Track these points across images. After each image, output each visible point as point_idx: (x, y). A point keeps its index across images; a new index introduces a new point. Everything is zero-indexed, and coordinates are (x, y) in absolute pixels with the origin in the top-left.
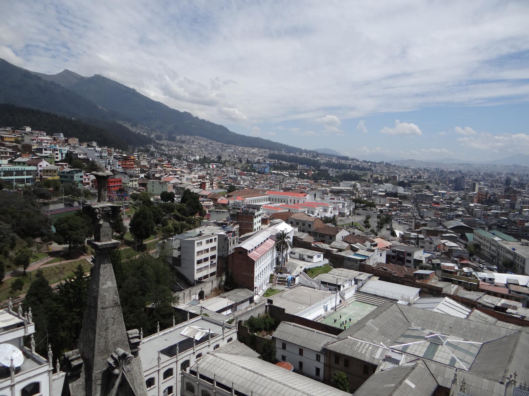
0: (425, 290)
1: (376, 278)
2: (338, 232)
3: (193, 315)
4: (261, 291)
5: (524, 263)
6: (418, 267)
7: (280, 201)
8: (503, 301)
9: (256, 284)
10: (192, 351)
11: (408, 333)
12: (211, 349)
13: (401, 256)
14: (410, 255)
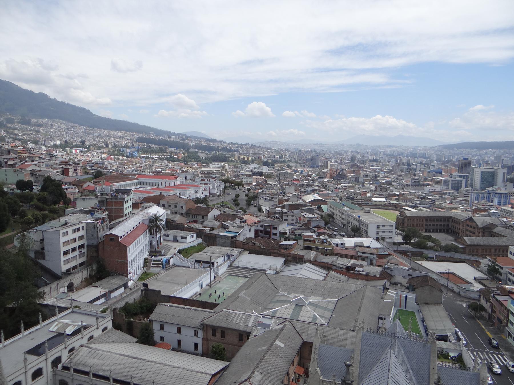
1: (247, 252)
2: (209, 212)
3: (62, 309)
4: (136, 276)
5: (367, 228)
6: (282, 239)
7: (151, 184)
8: (353, 261)
9: (129, 269)
10: (63, 346)
11: (276, 299)
12: (84, 341)
13: (268, 230)
14: (275, 228)
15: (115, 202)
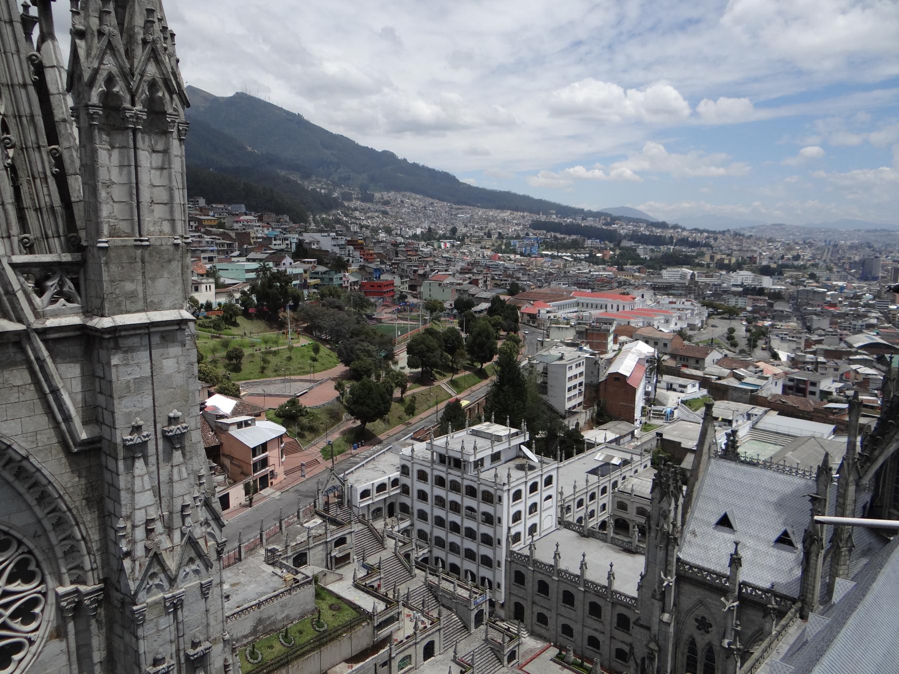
0: (842, 427)
1: (775, 413)
2: (707, 354)
12: (632, 474)
14: (814, 384)
15: (597, 334)
